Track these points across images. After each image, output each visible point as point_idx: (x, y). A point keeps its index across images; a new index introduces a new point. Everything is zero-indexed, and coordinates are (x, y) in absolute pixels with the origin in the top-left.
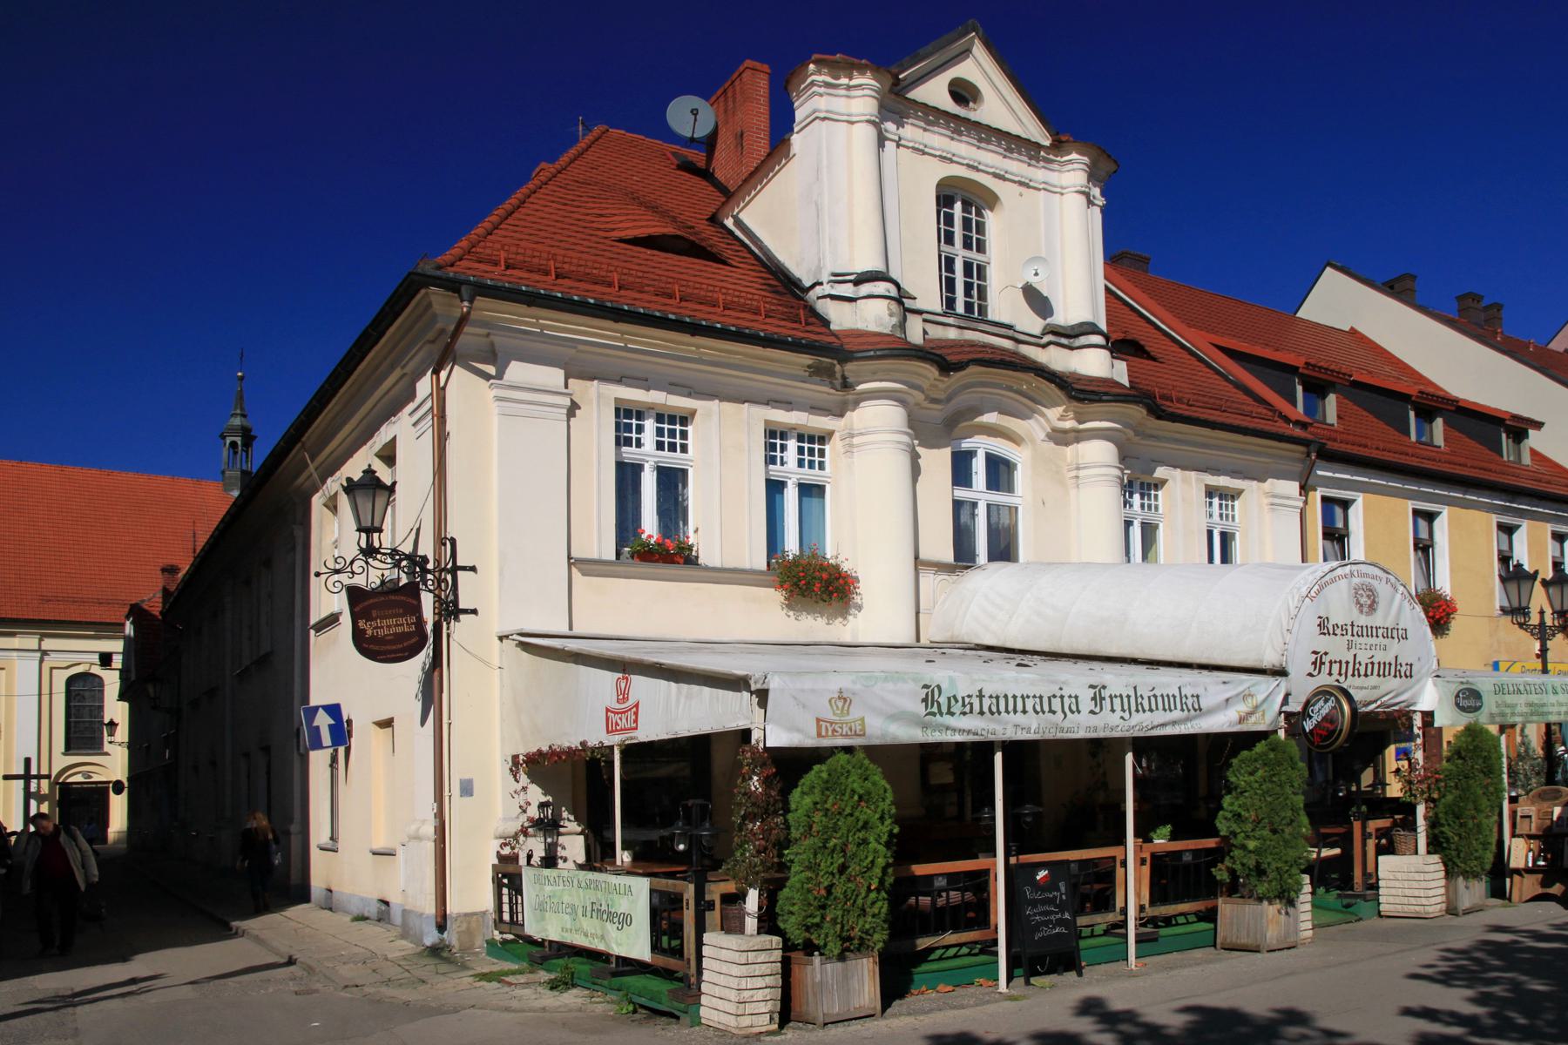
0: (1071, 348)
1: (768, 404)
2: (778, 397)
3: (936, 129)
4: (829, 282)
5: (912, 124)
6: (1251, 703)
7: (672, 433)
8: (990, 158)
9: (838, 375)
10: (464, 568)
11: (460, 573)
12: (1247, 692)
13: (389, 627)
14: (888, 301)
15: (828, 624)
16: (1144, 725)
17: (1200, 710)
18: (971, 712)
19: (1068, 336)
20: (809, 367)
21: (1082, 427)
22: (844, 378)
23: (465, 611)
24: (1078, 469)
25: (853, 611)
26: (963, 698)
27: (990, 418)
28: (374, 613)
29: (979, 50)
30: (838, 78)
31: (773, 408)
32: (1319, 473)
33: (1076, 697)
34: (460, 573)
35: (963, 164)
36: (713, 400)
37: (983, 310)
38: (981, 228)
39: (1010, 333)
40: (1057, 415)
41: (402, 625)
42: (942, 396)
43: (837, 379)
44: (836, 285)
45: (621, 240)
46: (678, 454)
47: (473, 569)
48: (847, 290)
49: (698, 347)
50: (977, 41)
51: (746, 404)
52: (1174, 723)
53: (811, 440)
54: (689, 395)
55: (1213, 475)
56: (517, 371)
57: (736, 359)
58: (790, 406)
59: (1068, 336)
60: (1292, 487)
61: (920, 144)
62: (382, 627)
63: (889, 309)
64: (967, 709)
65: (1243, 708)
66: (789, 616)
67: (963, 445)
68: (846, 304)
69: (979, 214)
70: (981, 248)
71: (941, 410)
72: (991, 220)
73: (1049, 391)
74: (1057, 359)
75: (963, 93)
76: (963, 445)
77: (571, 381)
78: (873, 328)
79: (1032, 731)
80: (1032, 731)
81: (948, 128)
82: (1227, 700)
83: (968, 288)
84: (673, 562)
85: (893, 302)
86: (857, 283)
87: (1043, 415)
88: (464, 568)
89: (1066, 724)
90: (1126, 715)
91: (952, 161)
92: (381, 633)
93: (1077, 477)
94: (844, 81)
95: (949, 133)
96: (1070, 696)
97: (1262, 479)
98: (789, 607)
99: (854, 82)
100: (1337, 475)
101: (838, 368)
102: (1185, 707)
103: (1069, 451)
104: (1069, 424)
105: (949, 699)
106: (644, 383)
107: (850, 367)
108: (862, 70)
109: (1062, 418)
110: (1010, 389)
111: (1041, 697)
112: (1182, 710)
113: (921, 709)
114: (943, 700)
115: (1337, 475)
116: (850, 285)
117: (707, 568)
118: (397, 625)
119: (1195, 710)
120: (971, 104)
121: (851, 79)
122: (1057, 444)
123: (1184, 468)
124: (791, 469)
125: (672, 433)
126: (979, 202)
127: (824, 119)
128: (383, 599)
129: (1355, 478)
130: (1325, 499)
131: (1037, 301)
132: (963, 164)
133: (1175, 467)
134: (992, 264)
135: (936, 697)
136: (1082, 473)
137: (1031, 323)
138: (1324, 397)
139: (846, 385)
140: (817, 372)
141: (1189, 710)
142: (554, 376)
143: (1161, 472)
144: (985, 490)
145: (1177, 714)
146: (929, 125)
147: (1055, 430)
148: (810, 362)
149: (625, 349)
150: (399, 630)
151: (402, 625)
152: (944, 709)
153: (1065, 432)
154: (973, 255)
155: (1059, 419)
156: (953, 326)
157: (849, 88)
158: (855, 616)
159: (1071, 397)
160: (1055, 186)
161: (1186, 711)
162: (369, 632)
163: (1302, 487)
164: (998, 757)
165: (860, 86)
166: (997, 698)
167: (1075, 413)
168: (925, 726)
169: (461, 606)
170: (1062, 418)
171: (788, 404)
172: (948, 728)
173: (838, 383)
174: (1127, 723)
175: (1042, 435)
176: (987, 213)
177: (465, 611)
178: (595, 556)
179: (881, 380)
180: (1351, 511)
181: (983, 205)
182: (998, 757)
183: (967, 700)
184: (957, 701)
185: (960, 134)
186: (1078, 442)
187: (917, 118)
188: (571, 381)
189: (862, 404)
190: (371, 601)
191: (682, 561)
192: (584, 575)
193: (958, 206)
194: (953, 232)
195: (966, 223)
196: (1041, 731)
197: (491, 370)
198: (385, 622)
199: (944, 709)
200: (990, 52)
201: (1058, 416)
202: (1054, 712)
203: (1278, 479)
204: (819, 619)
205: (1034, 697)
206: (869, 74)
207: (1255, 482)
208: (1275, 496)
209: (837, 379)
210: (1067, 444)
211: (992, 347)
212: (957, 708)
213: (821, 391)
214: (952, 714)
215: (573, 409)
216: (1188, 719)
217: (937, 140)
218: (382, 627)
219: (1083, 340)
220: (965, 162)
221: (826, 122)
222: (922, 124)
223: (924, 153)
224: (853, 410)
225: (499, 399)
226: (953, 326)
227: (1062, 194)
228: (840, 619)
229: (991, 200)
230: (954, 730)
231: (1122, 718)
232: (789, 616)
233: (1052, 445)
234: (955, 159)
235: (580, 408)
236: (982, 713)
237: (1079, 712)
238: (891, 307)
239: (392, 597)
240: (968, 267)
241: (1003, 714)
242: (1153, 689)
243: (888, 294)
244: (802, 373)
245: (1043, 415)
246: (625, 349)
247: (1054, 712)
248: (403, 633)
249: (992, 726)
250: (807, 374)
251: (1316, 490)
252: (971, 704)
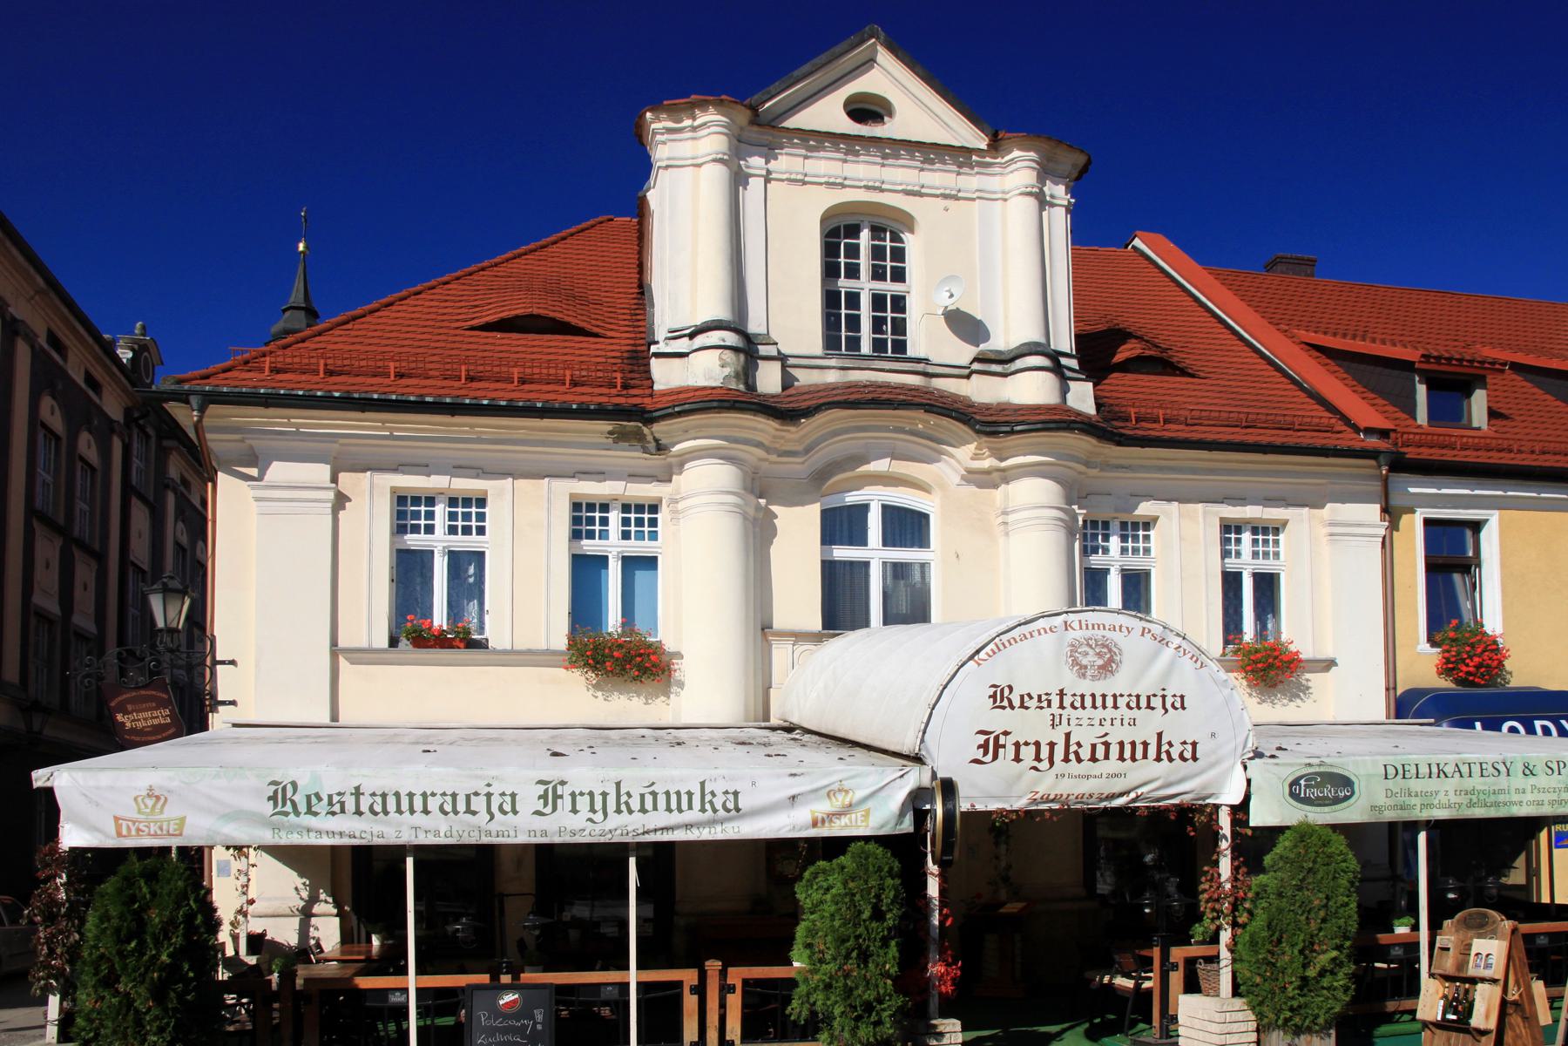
0: (1004, 375)
1: (574, 477)
2: (584, 468)
3: (822, 154)
4: (666, 339)
5: (786, 154)
6: (840, 801)
7: (467, 517)
8: (901, 173)
9: (650, 438)
10: (223, 663)
11: (219, 667)
12: (835, 787)
13: (145, 719)
14: (720, 351)
15: (646, 703)
16: (630, 829)
17: (738, 810)
18: (343, 811)
19: (1000, 363)
20: (610, 433)
21: (1004, 464)
22: (656, 440)
23: (223, 703)
24: (1005, 513)
25: (674, 689)
26: (330, 797)
27: (880, 466)
28: (130, 707)
29: (884, 57)
30: (681, 121)
31: (580, 480)
32: (1412, 490)
33: (513, 796)
34: (219, 667)
35: (860, 187)
36: (505, 479)
37: (900, 347)
38: (899, 254)
39: (920, 367)
40: (967, 453)
41: (156, 717)
42: (800, 448)
43: (649, 442)
44: (672, 341)
45: (472, 328)
46: (474, 537)
47: (233, 662)
48: (682, 345)
49: (472, 426)
50: (879, 48)
51: (547, 480)
52: (689, 826)
53: (640, 508)
54: (477, 477)
55: (1234, 506)
56: (279, 471)
57: (521, 435)
58: (601, 476)
59: (1000, 363)
60: (1372, 511)
61: (797, 174)
62: (139, 720)
63: (720, 359)
64: (337, 808)
65: (823, 807)
66: (596, 697)
67: (847, 499)
68: (677, 361)
69: (896, 238)
70: (899, 275)
71: (803, 463)
72: (911, 242)
73: (954, 428)
74: (983, 390)
75: (866, 110)
76: (847, 499)
77: (342, 476)
78: (702, 382)
79: (442, 834)
80: (442, 834)
81: (838, 150)
82: (794, 797)
83: (878, 324)
84: (452, 647)
85: (727, 351)
86: (692, 336)
87: (952, 456)
88: (223, 663)
89: (493, 826)
90: (599, 817)
91: (843, 186)
92: (140, 725)
93: (1005, 523)
94: (687, 123)
95: (841, 156)
96: (503, 794)
97: (1317, 504)
98: (597, 687)
99: (697, 123)
100: (1444, 491)
101: (646, 430)
102: (708, 806)
103: (998, 494)
104: (988, 463)
105: (309, 798)
106: (424, 468)
107: (658, 428)
108: (703, 106)
109: (975, 457)
110: (901, 430)
111: (454, 796)
112: (703, 810)
113: (268, 808)
114: (300, 799)
115: (1444, 491)
116: (686, 339)
117: (495, 652)
118: (153, 718)
119: (728, 811)
120: (886, 119)
121: (694, 119)
122: (980, 487)
123: (1182, 500)
124: (612, 545)
125: (467, 517)
126: (895, 226)
127: (667, 167)
128: (134, 694)
129: (1477, 492)
130: (1428, 522)
131: (964, 325)
132: (860, 187)
133: (1169, 500)
134: (913, 292)
135: (289, 794)
136: (1010, 518)
137: (962, 353)
138: (1469, 395)
139: (661, 448)
140: (620, 437)
141: (715, 811)
142: (322, 472)
143: (1145, 509)
144: (881, 547)
145: (693, 815)
146: (811, 151)
147: (970, 472)
148: (610, 428)
149: (392, 437)
150: (156, 722)
151: (156, 717)
152: (302, 808)
153: (987, 472)
154: (889, 287)
155: (972, 459)
156: (833, 368)
157: (694, 129)
158: (677, 694)
159: (978, 432)
160: (995, 193)
161: (710, 813)
162: (128, 725)
163: (1385, 510)
164: (410, 862)
165: (705, 124)
166: (384, 796)
167: (990, 449)
168: (276, 828)
169: (220, 698)
170: (975, 457)
171: (600, 475)
172: (309, 831)
173: (652, 446)
174: (598, 828)
175: (957, 480)
176: (906, 236)
177: (223, 703)
178: (364, 644)
179: (695, 439)
180: (1483, 535)
181: (901, 228)
182: (410, 862)
183: (336, 799)
184: (320, 799)
185: (857, 154)
186: (1007, 483)
187: (794, 146)
188: (342, 476)
189: (686, 467)
190: (124, 696)
191: (462, 645)
192: (352, 663)
193: (865, 235)
194: (859, 265)
195: (878, 253)
196: (455, 833)
197: (254, 472)
198: (141, 716)
199: (302, 808)
200: (897, 56)
201: (971, 455)
202: (474, 813)
203: (1343, 502)
204: (636, 699)
205: (444, 794)
206: (711, 109)
207: (1306, 509)
208: (1332, 524)
209: (649, 442)
210: (996, 486)
211: (887, 386)
212: (322, 807)
213: (631, 457)
214: (315, 814)
215: (341, 501)
216: (711, 823)
217: (825, 165)
218: (139, 720)
219: (1019, 364)
220: (862, 184)
221: (670, 170)
222: (803, 152)
223: (805, 183)
224: (681, 473)
225: (258, 499)
226: (833, 368)
227: (1005, 200)
228: (663, 698)
229: (908, 222)
230: (319, 832)
231: (590, 820)
232: (596, 697)
233: (974, 489)
234: (847, 182)
235: (350, 500)
236: (359, 813)
237: (515, 812)
238: (724, 357)
239: (143, 692)
240: (878, 301)
241: (393, 815)
242: (653, 784)
243: (722, 343)
244: (605, 441)
245: (952, 456)
246: (392, 437)
247: (474, 813)
248: (160, 724)
249: (377, 829)
250: (610, 440)
251: (1413, 512)
252: (342, 804)
